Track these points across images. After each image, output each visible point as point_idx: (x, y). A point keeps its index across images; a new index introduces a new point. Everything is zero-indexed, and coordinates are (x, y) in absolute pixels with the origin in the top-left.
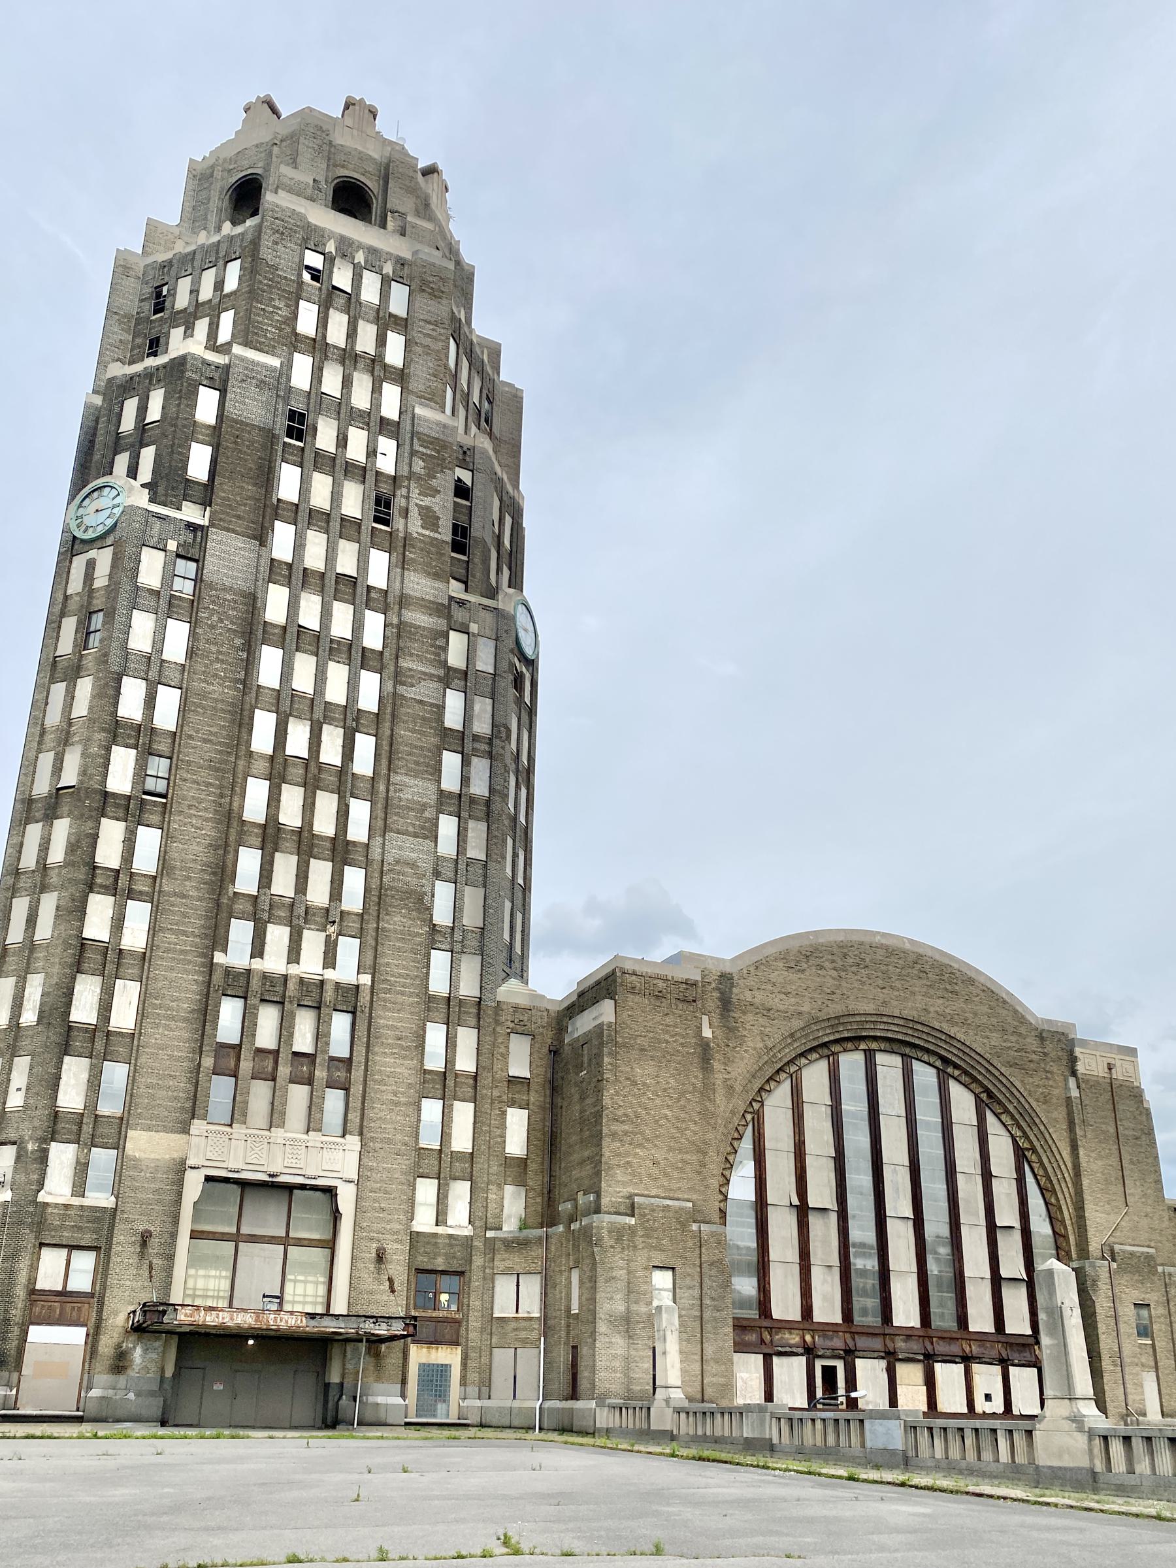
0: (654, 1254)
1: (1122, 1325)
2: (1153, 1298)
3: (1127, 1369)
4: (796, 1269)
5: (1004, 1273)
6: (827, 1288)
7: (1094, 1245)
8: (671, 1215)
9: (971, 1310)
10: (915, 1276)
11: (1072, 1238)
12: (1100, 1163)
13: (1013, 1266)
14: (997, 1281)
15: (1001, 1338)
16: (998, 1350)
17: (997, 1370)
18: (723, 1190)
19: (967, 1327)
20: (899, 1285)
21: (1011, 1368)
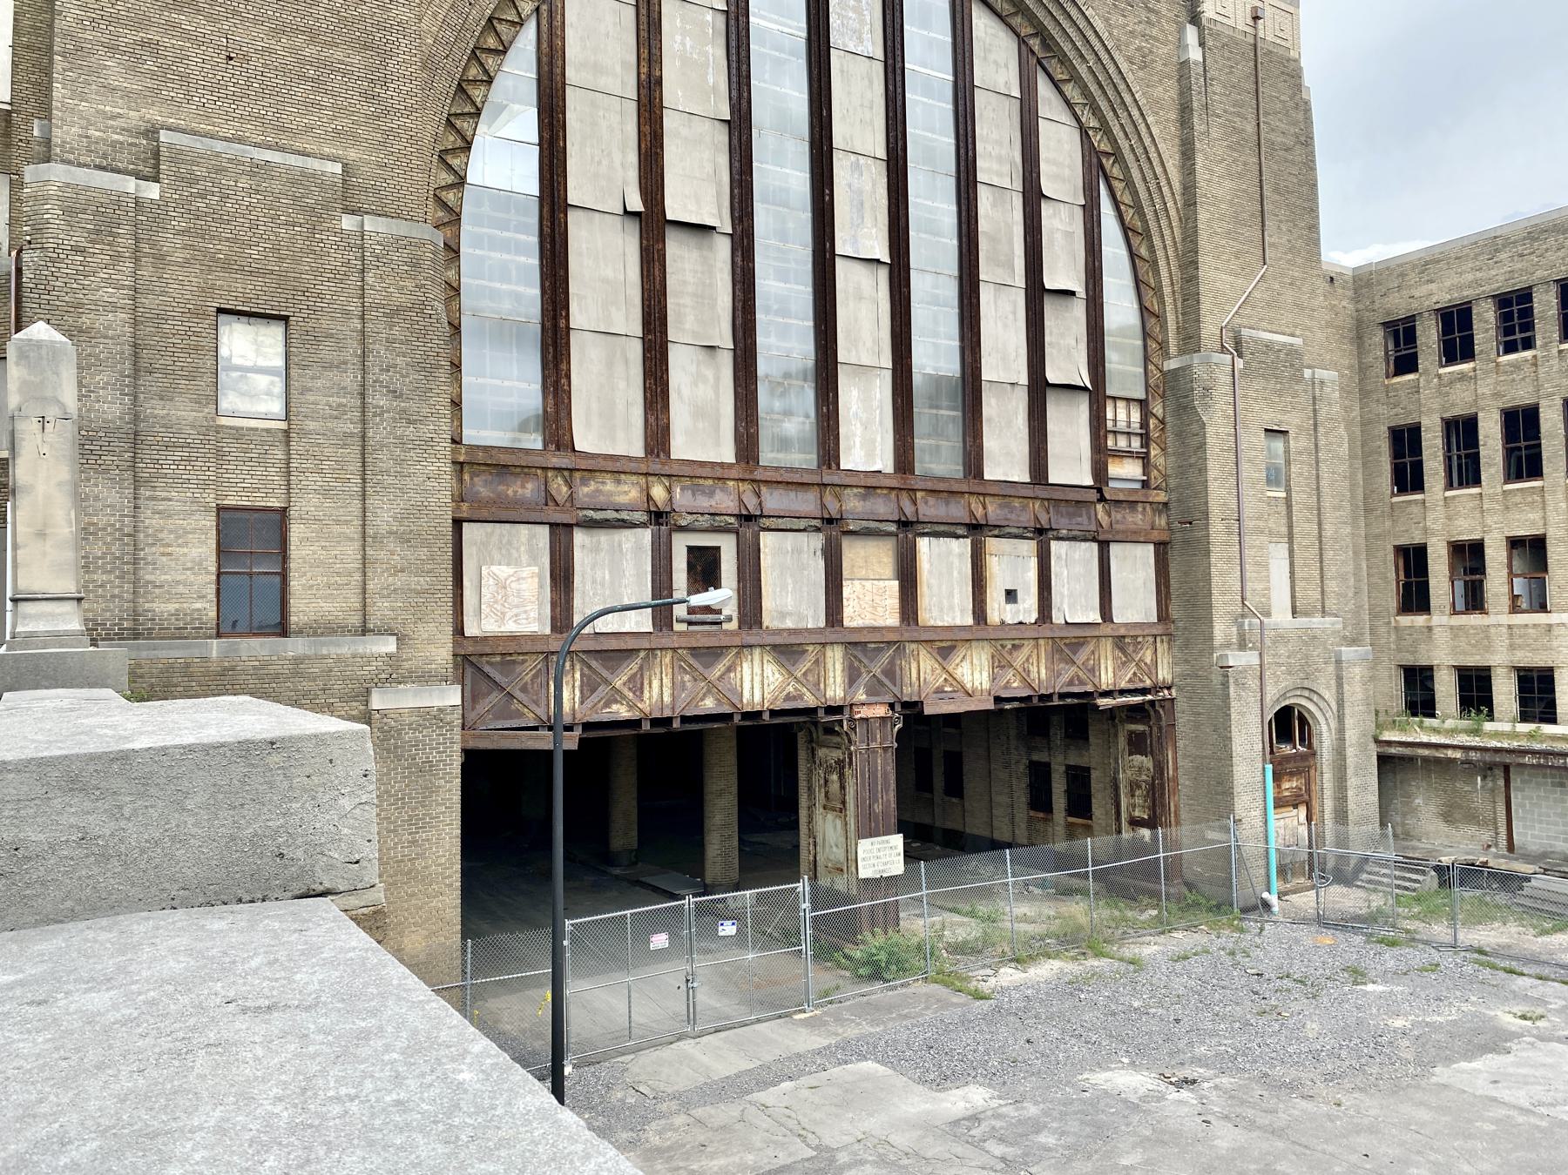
0: (220, 279)
1: (1244, 466)
2: (1292, 421)
3: (1247, 539)
4: (635, 350)
5: (1052, 376)
6: (704, 392)
7: (1209, 329)
8: (277, 186)
9: (990, 442)
10: (888, 375)
11: (1171, 318)
12: (1227, 184)
13: (1067, 362)
14: (1039, 389)
15: (1040, 492)
16: (1026, 514)
17: (1028, 548)
18: (455, 162)
19: (979, 474)
20: (855, 393)
21: (1053, 543)
